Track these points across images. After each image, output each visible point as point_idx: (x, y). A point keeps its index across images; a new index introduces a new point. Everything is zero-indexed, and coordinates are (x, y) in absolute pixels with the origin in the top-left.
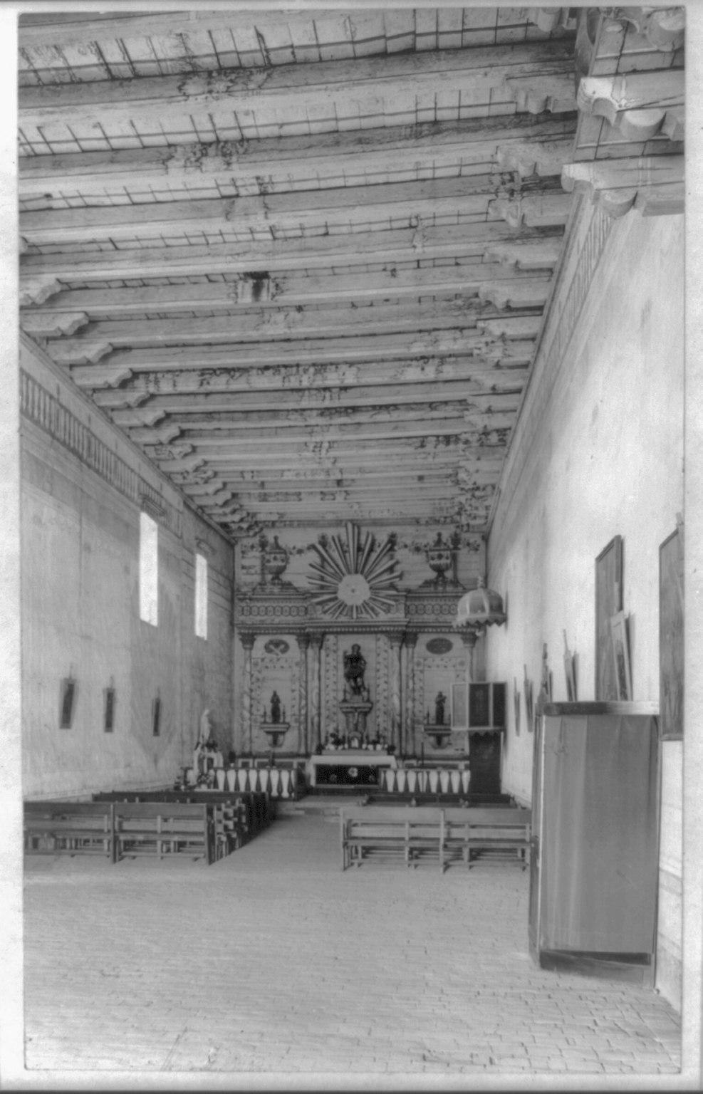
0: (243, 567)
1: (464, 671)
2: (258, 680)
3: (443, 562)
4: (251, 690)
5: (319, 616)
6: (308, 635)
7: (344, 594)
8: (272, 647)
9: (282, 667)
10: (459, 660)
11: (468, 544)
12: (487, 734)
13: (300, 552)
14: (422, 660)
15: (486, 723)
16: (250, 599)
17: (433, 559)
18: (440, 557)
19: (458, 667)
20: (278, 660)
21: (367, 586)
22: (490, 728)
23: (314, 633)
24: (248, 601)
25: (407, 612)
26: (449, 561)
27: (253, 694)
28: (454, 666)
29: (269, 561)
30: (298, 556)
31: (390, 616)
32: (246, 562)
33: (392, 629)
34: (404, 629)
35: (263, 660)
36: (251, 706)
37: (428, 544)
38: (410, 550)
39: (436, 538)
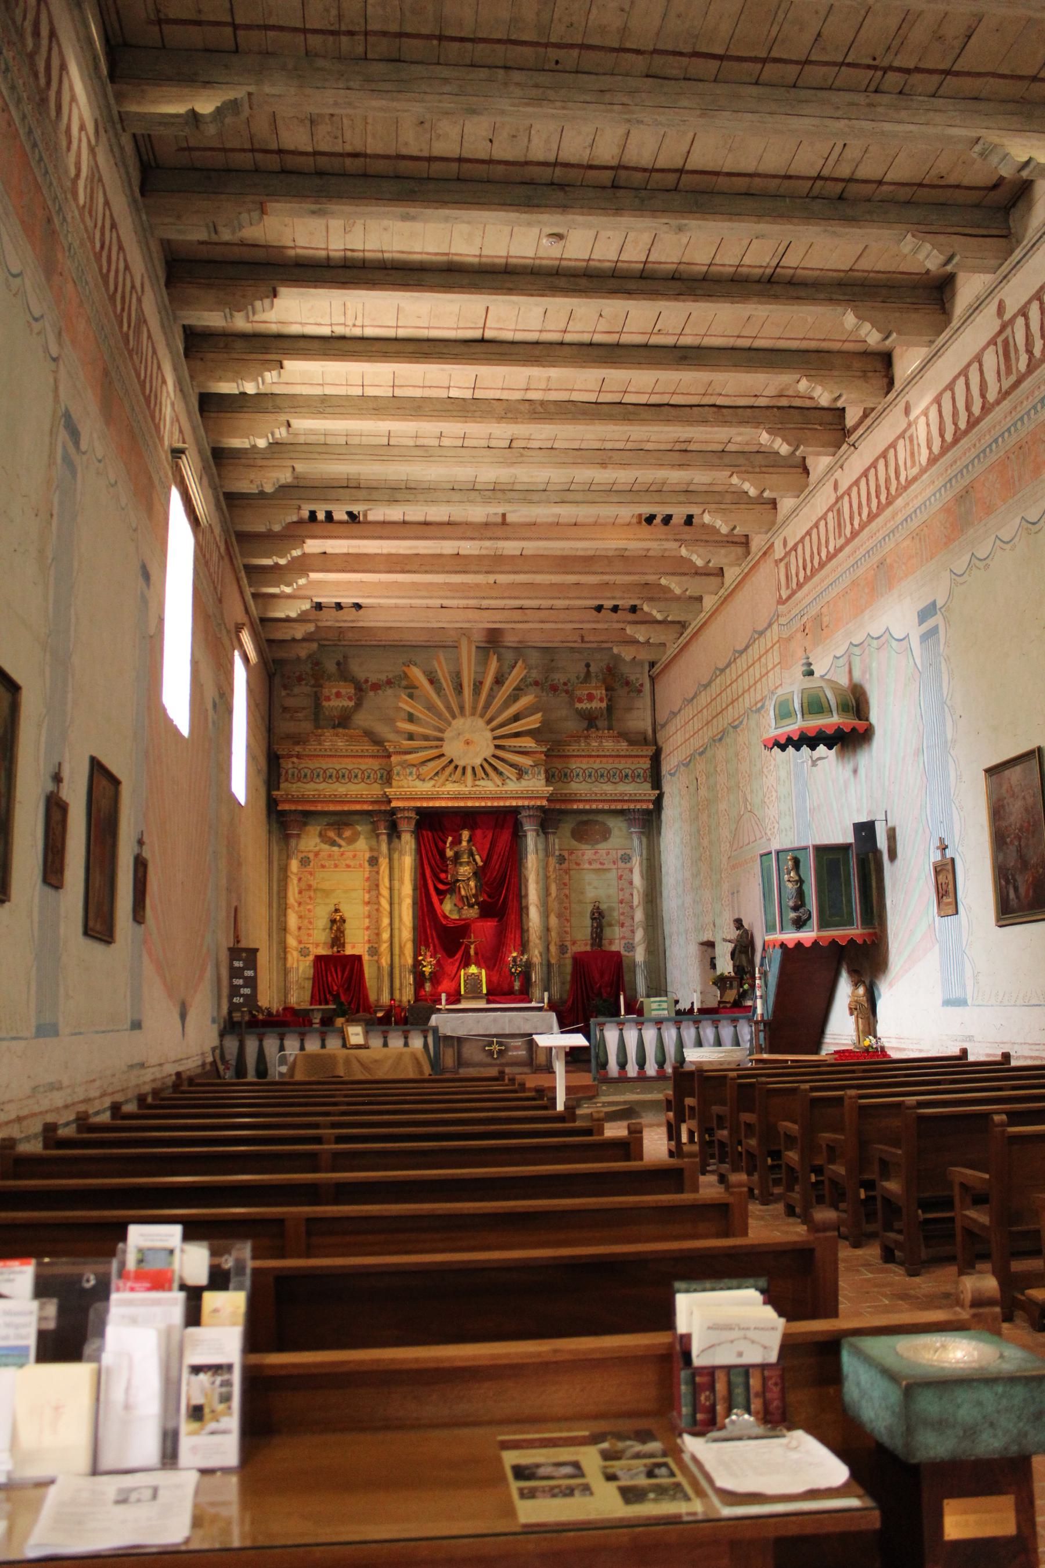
0: (285, 709)
1: (631, 871)
2: (310, 887)
3: (595, 704)
4: (300, 904)
5: (412, 783)
6: (393, 812)
7: (453, 749)
8: (331, 834)
9: (348, 866)
10: (621, 852)
11: (627, 683)
12: (852, 941)
13: (376, 687)
14: (566, 854)
15: (850, 923)
16: (298, 756)
17: (580, 701)
18: (591, 697)
19: (621, 865)
21: (489, 735)
22: (855, 931)
23: (404, 809)
24: (295, 760)
25: (548, 780)
26: (604, 705)
27: (302, 908)
28: (614, 863)
29: (328, 699)
30: (372, 694)
31: (524, 783)
32: (290, 702)
33: (526, 803)
34: (545, 803)
35: (317, 854)
36: (300, 928)
37: (569, 681)
38: (543, 690)
39: (583, 671)
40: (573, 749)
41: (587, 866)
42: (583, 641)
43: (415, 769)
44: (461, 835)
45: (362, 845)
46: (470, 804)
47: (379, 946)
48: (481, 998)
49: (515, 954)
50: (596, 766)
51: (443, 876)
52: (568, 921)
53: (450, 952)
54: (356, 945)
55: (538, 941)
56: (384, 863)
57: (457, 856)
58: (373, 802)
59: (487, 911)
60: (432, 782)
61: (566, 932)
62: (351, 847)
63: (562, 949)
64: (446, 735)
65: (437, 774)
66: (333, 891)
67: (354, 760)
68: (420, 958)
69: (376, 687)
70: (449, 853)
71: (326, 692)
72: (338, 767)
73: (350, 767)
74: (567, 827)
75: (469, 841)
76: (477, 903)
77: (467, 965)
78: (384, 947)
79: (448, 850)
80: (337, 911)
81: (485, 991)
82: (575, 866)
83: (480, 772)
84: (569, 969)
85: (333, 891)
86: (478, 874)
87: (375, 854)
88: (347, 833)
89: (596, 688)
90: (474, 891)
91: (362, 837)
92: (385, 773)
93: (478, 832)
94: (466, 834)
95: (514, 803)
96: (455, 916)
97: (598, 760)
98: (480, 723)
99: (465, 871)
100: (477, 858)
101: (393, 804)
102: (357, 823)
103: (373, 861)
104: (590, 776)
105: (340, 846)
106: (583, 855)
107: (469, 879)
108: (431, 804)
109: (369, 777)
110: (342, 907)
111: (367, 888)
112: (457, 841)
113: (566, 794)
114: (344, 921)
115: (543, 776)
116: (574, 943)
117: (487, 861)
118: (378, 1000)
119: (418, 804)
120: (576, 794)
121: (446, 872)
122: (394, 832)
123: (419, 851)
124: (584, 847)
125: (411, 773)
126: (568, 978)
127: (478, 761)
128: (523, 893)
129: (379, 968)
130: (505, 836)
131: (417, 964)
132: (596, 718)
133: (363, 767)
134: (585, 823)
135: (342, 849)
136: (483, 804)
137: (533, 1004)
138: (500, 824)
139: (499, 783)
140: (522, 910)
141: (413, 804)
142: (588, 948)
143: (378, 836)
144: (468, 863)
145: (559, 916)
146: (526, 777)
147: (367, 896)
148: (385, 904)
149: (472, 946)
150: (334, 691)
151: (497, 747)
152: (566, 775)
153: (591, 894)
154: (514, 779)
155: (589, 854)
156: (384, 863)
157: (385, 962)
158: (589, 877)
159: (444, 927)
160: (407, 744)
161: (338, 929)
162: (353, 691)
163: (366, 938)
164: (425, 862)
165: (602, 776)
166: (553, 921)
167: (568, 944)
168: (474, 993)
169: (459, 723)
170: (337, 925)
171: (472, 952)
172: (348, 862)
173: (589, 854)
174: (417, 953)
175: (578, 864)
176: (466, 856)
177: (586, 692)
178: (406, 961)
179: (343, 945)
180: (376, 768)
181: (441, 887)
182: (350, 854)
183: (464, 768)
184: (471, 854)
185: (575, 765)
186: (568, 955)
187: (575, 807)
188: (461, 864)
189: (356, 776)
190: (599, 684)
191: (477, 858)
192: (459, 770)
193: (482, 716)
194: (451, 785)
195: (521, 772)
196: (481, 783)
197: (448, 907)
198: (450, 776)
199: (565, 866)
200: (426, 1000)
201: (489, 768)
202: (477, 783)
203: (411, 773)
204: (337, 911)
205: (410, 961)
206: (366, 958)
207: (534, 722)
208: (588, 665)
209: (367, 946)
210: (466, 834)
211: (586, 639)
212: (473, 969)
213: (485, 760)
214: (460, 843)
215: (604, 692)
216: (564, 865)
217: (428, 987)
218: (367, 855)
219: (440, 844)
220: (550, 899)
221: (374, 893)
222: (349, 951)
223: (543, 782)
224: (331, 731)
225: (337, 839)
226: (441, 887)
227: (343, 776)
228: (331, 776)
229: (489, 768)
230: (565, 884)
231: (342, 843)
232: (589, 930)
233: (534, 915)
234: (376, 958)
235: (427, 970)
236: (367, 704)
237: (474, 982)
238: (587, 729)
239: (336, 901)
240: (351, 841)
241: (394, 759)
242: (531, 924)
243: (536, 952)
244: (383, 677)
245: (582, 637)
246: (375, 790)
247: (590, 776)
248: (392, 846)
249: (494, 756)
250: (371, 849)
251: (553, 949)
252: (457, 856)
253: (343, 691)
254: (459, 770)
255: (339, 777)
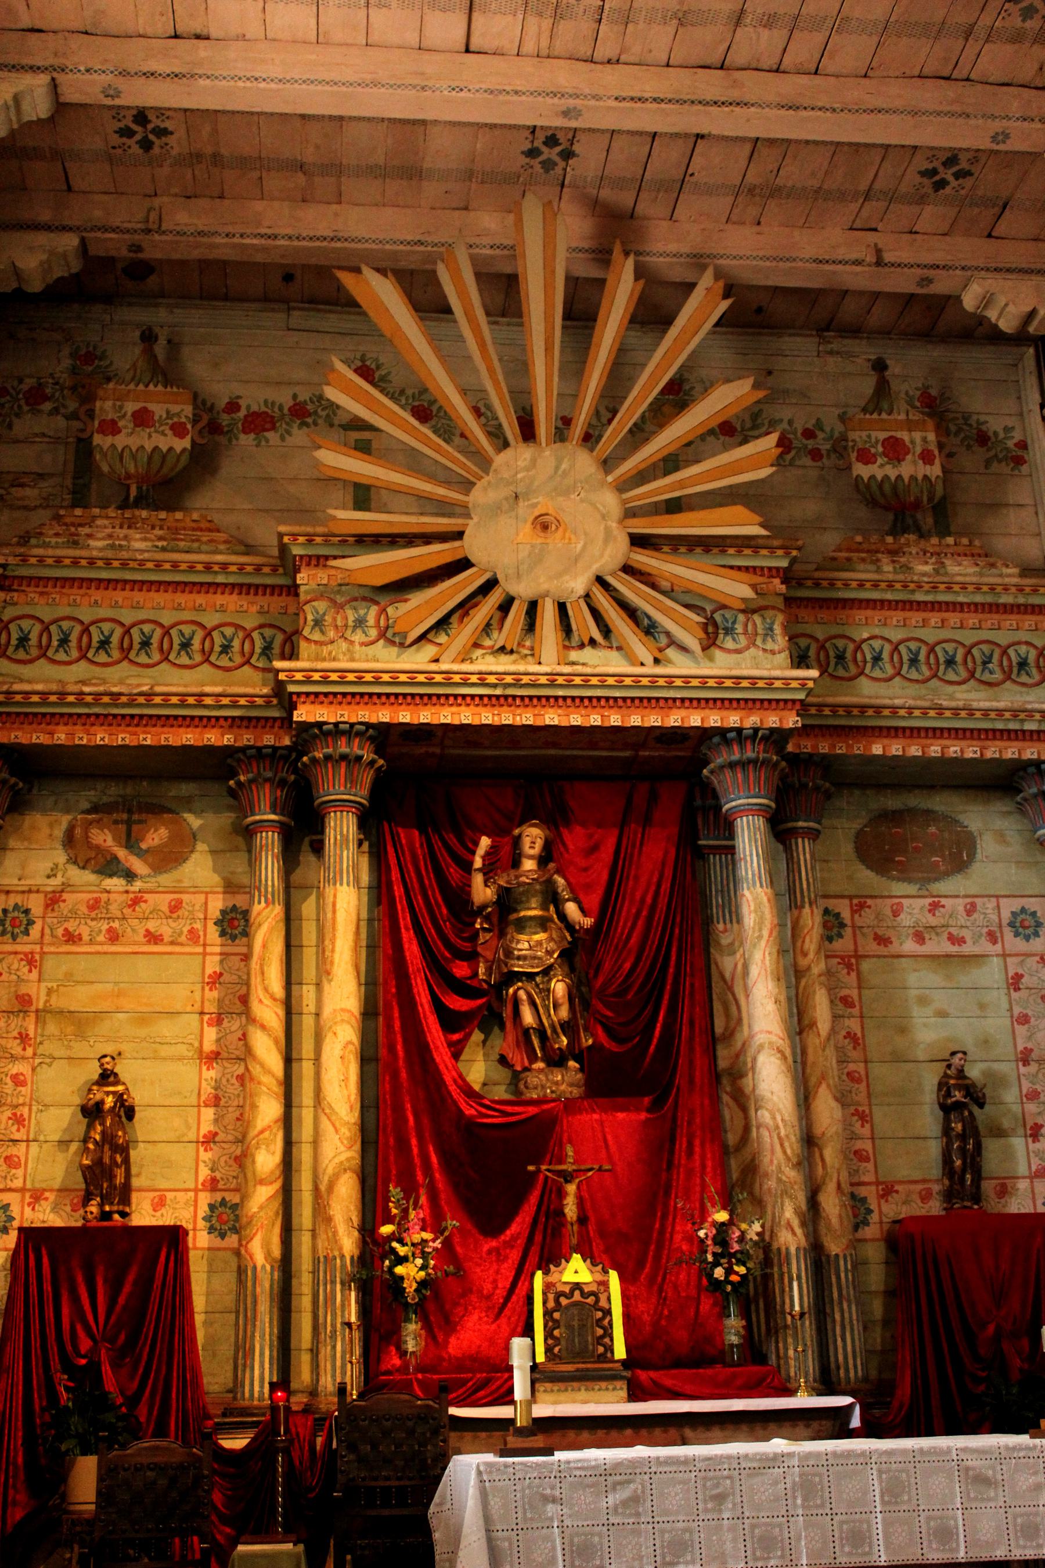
3: (909, 469)
7: (496, 542)
8: (104, 838)
9: (153, 938)
13: (260, 423)
14: (844, 909)
17: (866, 457)
18: (895, 450)
20: (136, 902)
21: (610, 502)
23: (337, 731)
26: (935, 471)
29: (111, 428)
30: (246, 440)
33: (733, 719)
34: (792, 720)
39: (867, 385)
40: (860, 577)
41: (909, 946)
42: (879, 263)
43: (374, 610)
44: (517, 841)
45: (200, 870)
46: (552, 717)
47: (245, 1198)
48: (613, 1378)
49: (722, 1216)
50: (930, 635)
51: (460, 970)
52: (863, 1118)
53: (489, 1219)
54: (167, 1190)
55: (791, 1174)
56: (267, 919)
57: (507, 903)
58: (234, 723)
59: (606, 1080)
60: (429, 651)
61: (860, 1156)
62: (165, 879)
63: (858, 1211)
64: (480, 496)
65: (442, 624)
66: (99, 1015)
67: (181, 598)
68: (386, 1229)
69: (260, 423)
70: (482, 892)
71: (105, 408)
72: (127, 617)
73: (167, 619)
74: (844, 827)
75: (543, 860)
76: (575, 1052)
77: (552, 1257)
78: (262, 1198)
79: (478, 879)
80: (107, 1077)
81: (620, 1352)
82: (872, 947)
83: (584, 624)
84: (876, 1277)
85: (99, 1015)
86: (577, 953)
87: (240, 901)
88: (156, 836)
89: (910, 426)
90: (564, 1013)
91: (201, 847)
92: (280, 638)
93: (575, 838)
94: (532, 838)
95: (695, 720)
96: (500, 1093)
97: (935, 618)
98: (584, 463)
99: (533, 946)
100: (571, 909)
101: (303, 714)
102: (187, 802)
103: (235, 924)
104: (914, 661)
105: (130, 876)
106: (896, 914)
107: (547, 972)
108: (426, 716)
109: (226, 649)
110: (121, 1069)
111: (211, 1008)
112: (506, 857)
113: (848, 708)
114: (130, 1113)
115: (781, 641)
116: (887, 1191)
117: (605, 913)
118: (236, 1386)
119: (384, 715)
120: (878, 709)
121: (472, 957)
122: (303, 832)
123: (380, 894)
124: (899, 888)
125: (360, 623)
126: (877, 1308)
127: (578, 584)
128: (719, 1027)
129: (241, 1271)
130: (655, 852)
131: (373, 1250)
132: (917, 505)
133: (210, 620)
134: (895, 817)
135: (138, 885)
136: (595, 720)
137: (803, 1400)
138: (643, 790)
139: (649, 659)
140: (723, 1080)
141: (365, 714)
142: (935, 1207)
143: (248, 833)
144: (543, 924)
145: (842, 1099)
146: (729, 644)
147: (211, 1034)
148: (268, 1053)
149: (571, 1188)
150: (131, 407)
151: (639, 541)
152: (841, 657)
153: (928, 1033)
154: (693, 644)
155: (914, 910)
156: (267, 919)
157: (261, 1249)
158: (919, 979)
159: (470, 1128)
160: (349, 518)
161: (108, 1138)
162: (188, 410)
163: (204, 1172)
164: (405, 920)
165: (950, 662)
166: (827, 1112)
167: (869, 1193)
168: (576, 1356)
169: (517, 460)
170: (107, 1121)
171: (571, 1210)
172: (152, 925)
173: (914, 910)
174: (372, 1209)
175: (883, 941)
176: (534, 902)
177: (882, 435)
178: (335, 1239)
179: (125, 1193)
180: (248, 625)
181: (457, 1003)
182: (163, 901)
183: (533, 607)
184: (552, 898)
185: (865, 628)
186: (871, 1231)
187: (877, 749)
188: (521, 925)
189: (186, 645)
190: (915, 416)
191: (571, 909)
192: (517, 612)
193: (589, 439)
194: (490, 659)
195: (712, 635)
196: (588, 655)
197: (477, 1068)
198: (487, 629)
199: (843, 945)
200: (406, 1387)
201: (608, 610)
202: (574, 655)
203: (360, 623)
204: (107, 1077)
205: (348, 1243)
206: (200, 1240)
207: (753, 463)
208: (880, 366)
209: (205, 1199)
210: (532, 838)
211: (888, 257)
212: (577, 1271)
213: (600, 580)
214: (516, 863)
215: (931, 437)
216: (836, 952)
217: (412, 1336)
218: (217, 904)
219: (453, 873)
220: (813, 1042)
221: (234, 1025)
222: (144, 1214)
223: (783, 658)
224: (112, 512)
225: (121, 853)
226: (457, 1003)
227: (146, 644)
228: (104, 644)
229: (608, 610)
230: (846, 1001)
231: (138, 865)
232: (934, 1149)
233: (771, 1081)
234: (232, 1240)
235: (410, 1272)
236: (230, 467)
237: (579, 1313)
238: (893, 532)
239: (109, 1049)
240: (168, 859)
241: (301, 578)
242: (765, 1116)
243: (789, 1213)
244: (284, 398)
245: (879, 252)
246: (250, 684)
247: (914, 661)
248: (296, 877)
249: (628, 569)
250: (230, 887)
251: (831, 1204)
252: (507, 903)
253: (158, 410)
254: (517, 612)
255: (131, 646)
